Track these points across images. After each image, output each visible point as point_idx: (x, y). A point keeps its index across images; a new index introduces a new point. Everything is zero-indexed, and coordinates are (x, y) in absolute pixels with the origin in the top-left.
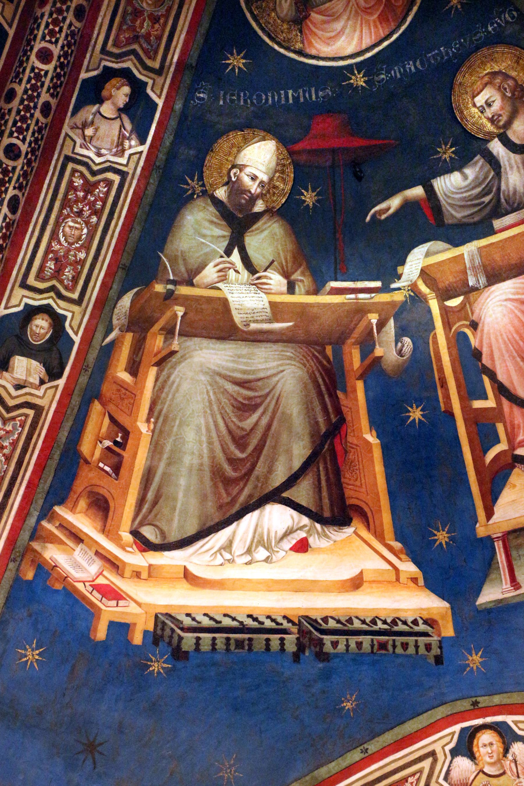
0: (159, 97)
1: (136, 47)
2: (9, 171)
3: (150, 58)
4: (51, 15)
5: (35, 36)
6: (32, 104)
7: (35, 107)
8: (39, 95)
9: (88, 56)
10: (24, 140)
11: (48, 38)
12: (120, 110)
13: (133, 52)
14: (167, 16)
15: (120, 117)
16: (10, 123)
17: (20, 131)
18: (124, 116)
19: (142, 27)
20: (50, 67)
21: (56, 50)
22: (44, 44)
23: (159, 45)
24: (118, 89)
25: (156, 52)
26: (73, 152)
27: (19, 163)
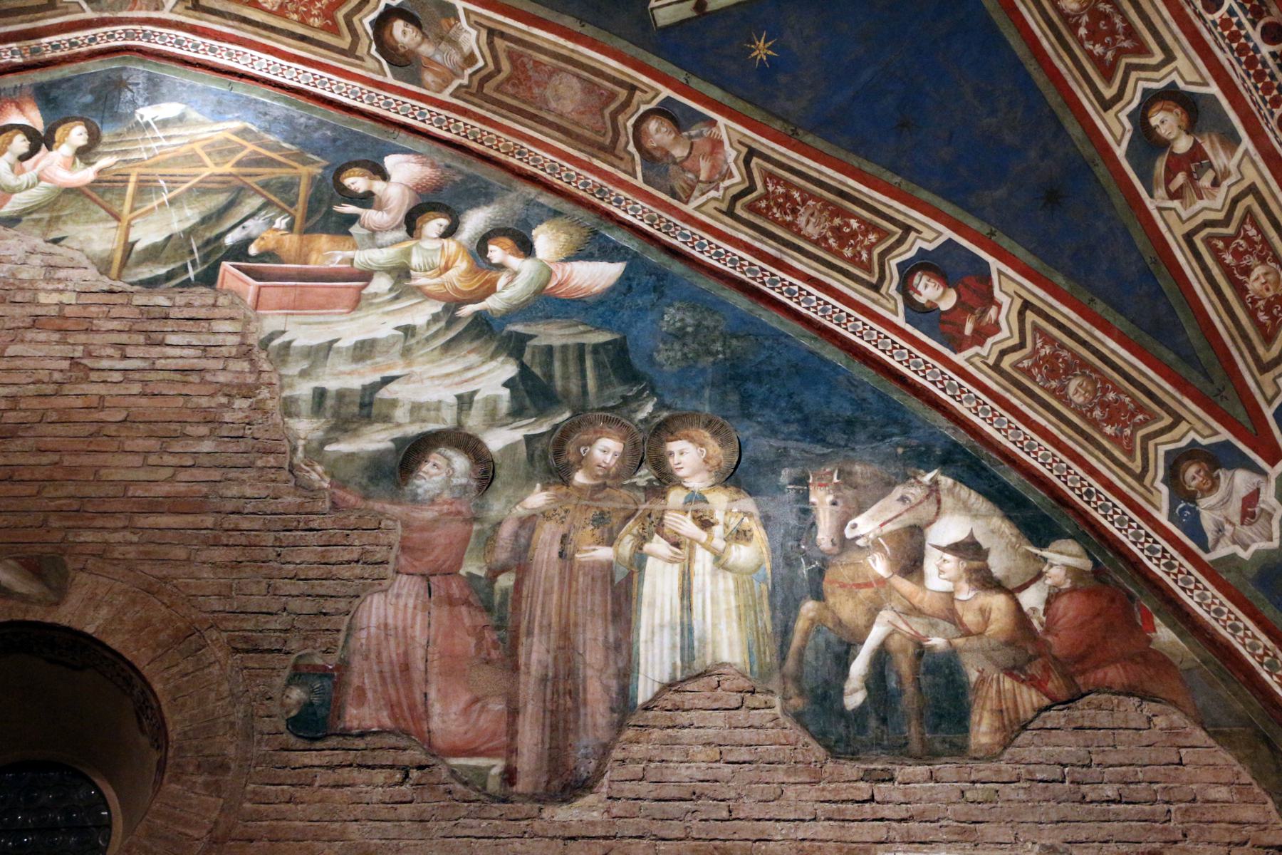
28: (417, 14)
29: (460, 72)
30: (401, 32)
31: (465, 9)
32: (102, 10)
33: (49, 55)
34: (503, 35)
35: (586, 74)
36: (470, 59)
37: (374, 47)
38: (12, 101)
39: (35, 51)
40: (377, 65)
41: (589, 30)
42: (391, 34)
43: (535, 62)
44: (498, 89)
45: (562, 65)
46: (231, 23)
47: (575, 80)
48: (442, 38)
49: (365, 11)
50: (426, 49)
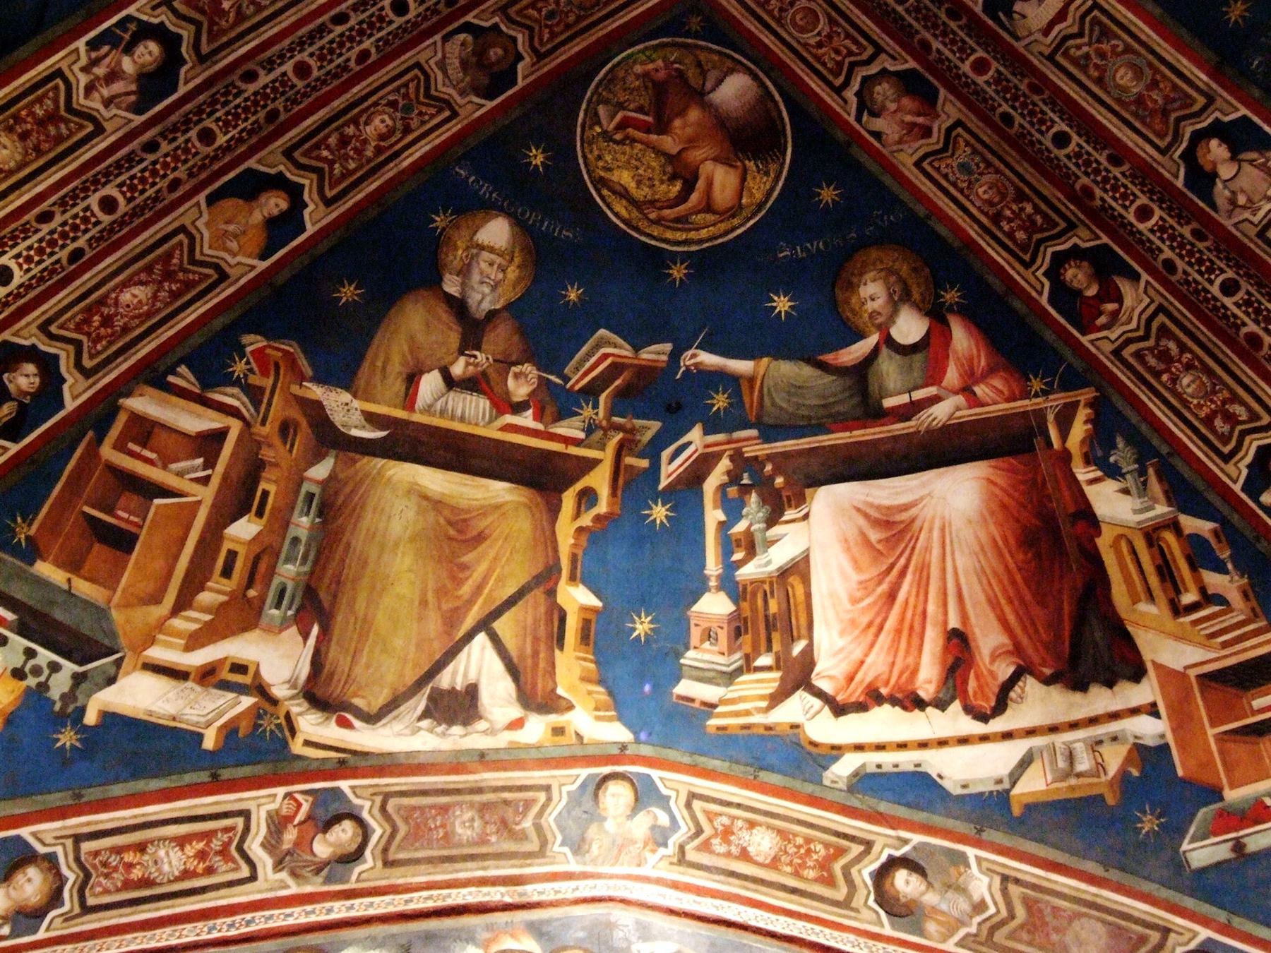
0: (1237, 110)
1: (1173, 116)
2: (1249, 300)
3: (1192, 105)
4: (1106, 191)
5: (1121, 216)
6: (1188, 247)
7: (1193, 245)
8: (1182, 236)
9: (1161, 170)
10: (1222, 271)
11: (1127, 203)
12: (1233, 158)
13: (1178, 120)
14: (1157, 71)
15: (1240, 161)
16: (1198, 278)
17: (1211, 270)
18: (1242, 156)
19: (1156, 101)
20: (1158, 213)
21: (1143, 200)
22: (1132, 209)
23: (1182, 90)
24: (1209, 151)
25: (1189, 96)
26: (1256, 226)
27: (1245, 285)
28: (921, 862)
29: (966, 918)
30: (904, 882)
31: (976, 857)
32: (585, 864)
33: (536, 898)
34: (1017, 881)
35: (1110, 918)
36: (980, 907)
37: (872, 897)
38: (506, 933)
39: (521, 895)
40: (874, 916)
41: (1114, 875)
42: (892, 884)
43: (1053, 908)
44: (1011, 936)
45: (1084, 910)
46: (716, 877)
47: (1099, 925)
48: (949, 887)
49: (866, 860)
50: (931, 898)
